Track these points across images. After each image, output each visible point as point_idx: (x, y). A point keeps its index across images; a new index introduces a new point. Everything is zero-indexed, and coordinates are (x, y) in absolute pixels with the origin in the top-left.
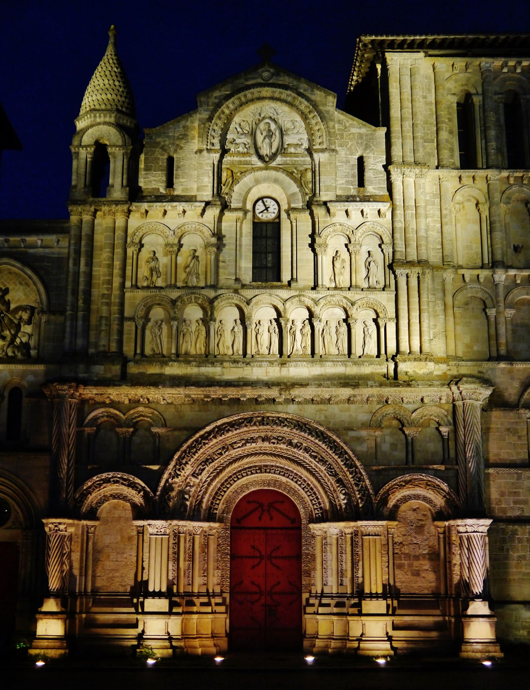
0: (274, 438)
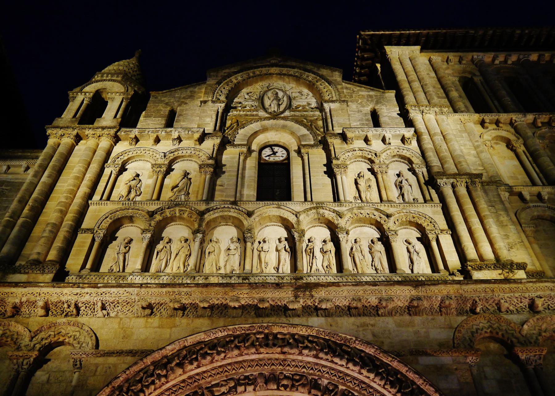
0: (286, 377)
